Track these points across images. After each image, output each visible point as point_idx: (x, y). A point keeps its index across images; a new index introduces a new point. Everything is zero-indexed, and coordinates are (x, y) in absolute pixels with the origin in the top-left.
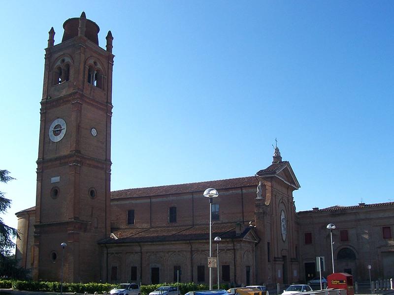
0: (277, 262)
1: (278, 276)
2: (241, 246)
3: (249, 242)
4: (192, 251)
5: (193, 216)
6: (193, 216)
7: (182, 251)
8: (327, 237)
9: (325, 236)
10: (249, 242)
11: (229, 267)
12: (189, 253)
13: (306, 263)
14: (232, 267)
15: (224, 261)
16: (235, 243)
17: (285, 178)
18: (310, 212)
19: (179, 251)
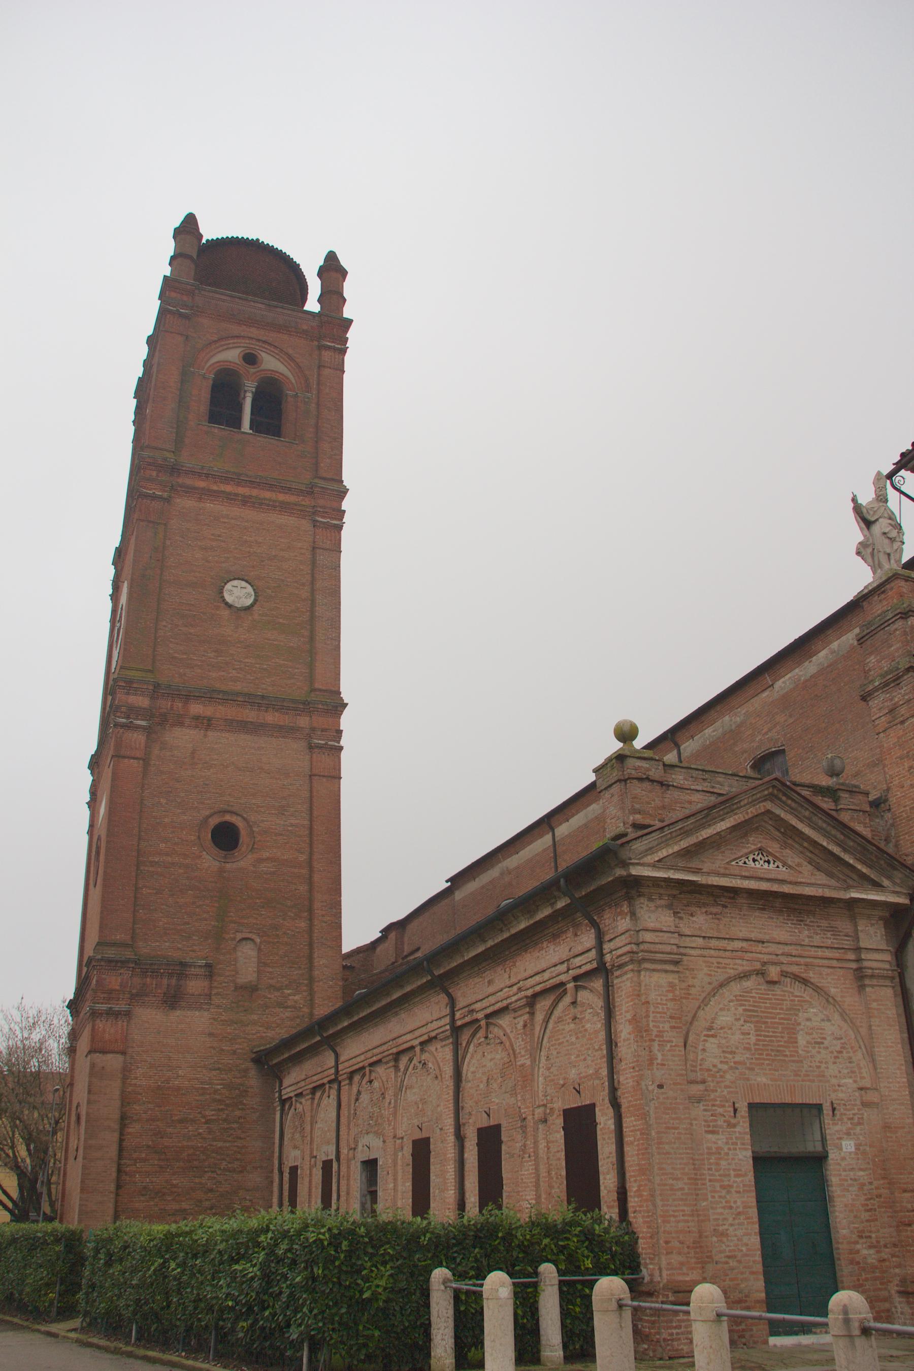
4: (456, 1031)
14: (605, 1120)
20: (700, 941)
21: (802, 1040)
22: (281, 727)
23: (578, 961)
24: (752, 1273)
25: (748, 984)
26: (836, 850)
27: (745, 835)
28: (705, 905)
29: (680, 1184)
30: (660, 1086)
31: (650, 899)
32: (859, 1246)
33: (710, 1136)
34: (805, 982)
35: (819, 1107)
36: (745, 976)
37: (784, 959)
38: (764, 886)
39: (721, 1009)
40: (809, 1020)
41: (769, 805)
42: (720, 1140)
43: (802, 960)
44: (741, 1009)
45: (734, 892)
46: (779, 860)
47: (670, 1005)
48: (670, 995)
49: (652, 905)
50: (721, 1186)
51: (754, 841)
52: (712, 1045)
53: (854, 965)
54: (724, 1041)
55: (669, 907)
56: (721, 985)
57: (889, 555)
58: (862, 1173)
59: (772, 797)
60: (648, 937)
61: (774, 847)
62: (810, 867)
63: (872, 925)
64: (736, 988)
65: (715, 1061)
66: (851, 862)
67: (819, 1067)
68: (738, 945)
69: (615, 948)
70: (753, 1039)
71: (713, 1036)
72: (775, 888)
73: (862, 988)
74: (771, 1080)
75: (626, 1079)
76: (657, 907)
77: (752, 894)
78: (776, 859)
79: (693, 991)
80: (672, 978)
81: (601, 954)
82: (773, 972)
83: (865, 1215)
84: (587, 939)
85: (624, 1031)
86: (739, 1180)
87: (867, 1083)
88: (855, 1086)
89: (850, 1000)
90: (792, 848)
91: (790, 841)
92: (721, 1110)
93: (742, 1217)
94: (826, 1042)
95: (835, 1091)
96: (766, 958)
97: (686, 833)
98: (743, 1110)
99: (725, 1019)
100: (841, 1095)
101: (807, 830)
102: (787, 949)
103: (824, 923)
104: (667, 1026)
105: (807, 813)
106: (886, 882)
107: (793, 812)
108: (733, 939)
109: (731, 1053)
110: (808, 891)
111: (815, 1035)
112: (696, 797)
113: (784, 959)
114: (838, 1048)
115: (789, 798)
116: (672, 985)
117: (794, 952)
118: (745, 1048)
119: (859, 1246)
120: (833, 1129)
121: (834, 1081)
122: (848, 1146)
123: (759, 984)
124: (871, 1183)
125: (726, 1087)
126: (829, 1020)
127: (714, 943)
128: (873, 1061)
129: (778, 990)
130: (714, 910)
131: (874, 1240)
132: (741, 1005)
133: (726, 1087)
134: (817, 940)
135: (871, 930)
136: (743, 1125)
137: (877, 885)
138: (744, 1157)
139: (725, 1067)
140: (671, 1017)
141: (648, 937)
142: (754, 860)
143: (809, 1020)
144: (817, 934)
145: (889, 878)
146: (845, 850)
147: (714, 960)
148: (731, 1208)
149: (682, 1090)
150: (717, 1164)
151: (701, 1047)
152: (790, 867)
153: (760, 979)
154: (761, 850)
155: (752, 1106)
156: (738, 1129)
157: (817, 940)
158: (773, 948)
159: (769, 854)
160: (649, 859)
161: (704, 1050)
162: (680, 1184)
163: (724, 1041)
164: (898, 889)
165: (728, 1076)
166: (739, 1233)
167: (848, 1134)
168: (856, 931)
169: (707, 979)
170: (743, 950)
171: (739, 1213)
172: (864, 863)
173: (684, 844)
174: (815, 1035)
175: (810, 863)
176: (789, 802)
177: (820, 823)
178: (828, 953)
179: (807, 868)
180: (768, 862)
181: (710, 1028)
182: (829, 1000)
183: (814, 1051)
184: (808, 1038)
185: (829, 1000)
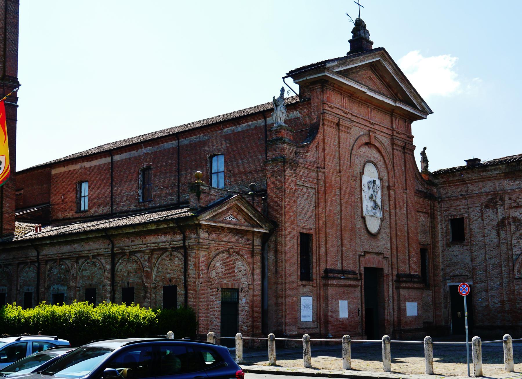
0: (331, 282)
1: (338, 312)
2: (199, 238)
3: (237, 232)
5: (178, 186)
6: (178, 186)
7: (98, 255)
8: (498, 225)
9: (495, 224)
10: (237, 232)
11: (176, 291)
12: (109, 261)
13: (450, 286)
14: (180, 290)
15: (168, 276)
16: (187, 233)
17: (384, 91)
18: (461, 169)
19: (94, 257)
21: (236, 271)
23: (174, 243)
24: (218, 333)
26: (252, 216)
28: (215, 231)
29: (204, 310)
30: (201, 283)
31: (203, 230)
32: (243, 326)
33: (211, 297)
34: (239, 254)
35: (238, 289)
36: (223, 252)
37: (234, 247)
38: (232, 226)
39: (217, 262)
40: (238, 265)
41: (236, 202)
42: (213, 298)
43: (238, 248)
44: (222, 262)
46: (236, 218)
47: (205, 260)
48: (205, 258)
49: (203, 231)
50: (213, 310)
52: (214, 272)
53: (251, 250)
54: (217, 271)
55: (207, 232)
57: (281, 118)
58: (246, 307)
59: (237, 200)
61: (235, 214)
62: (244, 220)
63: (258, 238)
64: (221, 255)
65: (214, 276)
66: (256, 220)
67: (239, 278)
68: (223, 243)
69: (190, 242)
70: (224, 270)
71: (214, 269)
73: (252, 256)
74: (228, 282)
75: (191, 280)
76: (204, 232)
77: (228, 228)
79: (211, 256)
80: (206, 253)
81: (184, 243)
82: (231, 251)
83: (246, 318)
84: (179, 237)
85: (191, 267)
86: (217, 308)
87: (250, 283)
88: (248, 284)
90: (240, 214)
91: (240, 213)
92: (214, 290)
93: (217, 318)
94: (242, 272)
95: (242, 285)
98: (220, 290)
100: (244, 286)
101: (245, 210)
102: (235, 244)
103: (245, 237)
104: (204, 266)
105: (246, 205)
106: (264, 226)
108: (222, 242)
109: (218, 274)
110: (243, 228)
111: (239, 270)
112: (217, 198)
113: (234, 247)
114: (245, 273)
115: (242, 200)
116: (206, 255)
117: (237, 246)
118: (222, 273)
119: (243, 326)
120: (241, 295)
121: (242, 282)
122: (244, 300)
123: (227, 255)
124: (248, 310)
125: (216, 283)
126: (243, 265)
127: (217, 242)
128: (253, 277)
130: (218, 233)
131: (247, 325)
132: (222, 261)
133: (216, 283)
134: (243, 241)
135: (257, 239)
136: (219, 294)
137: (261, 227)
138: (219, 302)
139: (216, 278)
140: (205, 264)
142: (230, 218)
143: (238, 265)
144: (243, 240)
145: (265, 225)
146: (254, 216)
147: (216, 247)
148: (215, 316)
149: (206, 284)
150: (212, 304)
151: (211, 272)
152: (239, 220)
154: (232, 215)
155: (222, 289)
156: (218, 295)
159: (234, 216)
161: (212, 273)
162: (204, 310)
163: (217, 271)
164: (267, 228)
165: (217, 281)
166: (216, 322)
167: (244, 297)
168: (253, 240)
169: (214, 253)
170: (224, 245)
171: (216, 317)
172: (259, 220)
174: (239, 270)
175: (244, 219)
176: (242, 202)
177: (249, 208)
179: (243, 220)
180: (233, 218)
181: (214, 267)
183: (238, 274)
184: (237, 270)
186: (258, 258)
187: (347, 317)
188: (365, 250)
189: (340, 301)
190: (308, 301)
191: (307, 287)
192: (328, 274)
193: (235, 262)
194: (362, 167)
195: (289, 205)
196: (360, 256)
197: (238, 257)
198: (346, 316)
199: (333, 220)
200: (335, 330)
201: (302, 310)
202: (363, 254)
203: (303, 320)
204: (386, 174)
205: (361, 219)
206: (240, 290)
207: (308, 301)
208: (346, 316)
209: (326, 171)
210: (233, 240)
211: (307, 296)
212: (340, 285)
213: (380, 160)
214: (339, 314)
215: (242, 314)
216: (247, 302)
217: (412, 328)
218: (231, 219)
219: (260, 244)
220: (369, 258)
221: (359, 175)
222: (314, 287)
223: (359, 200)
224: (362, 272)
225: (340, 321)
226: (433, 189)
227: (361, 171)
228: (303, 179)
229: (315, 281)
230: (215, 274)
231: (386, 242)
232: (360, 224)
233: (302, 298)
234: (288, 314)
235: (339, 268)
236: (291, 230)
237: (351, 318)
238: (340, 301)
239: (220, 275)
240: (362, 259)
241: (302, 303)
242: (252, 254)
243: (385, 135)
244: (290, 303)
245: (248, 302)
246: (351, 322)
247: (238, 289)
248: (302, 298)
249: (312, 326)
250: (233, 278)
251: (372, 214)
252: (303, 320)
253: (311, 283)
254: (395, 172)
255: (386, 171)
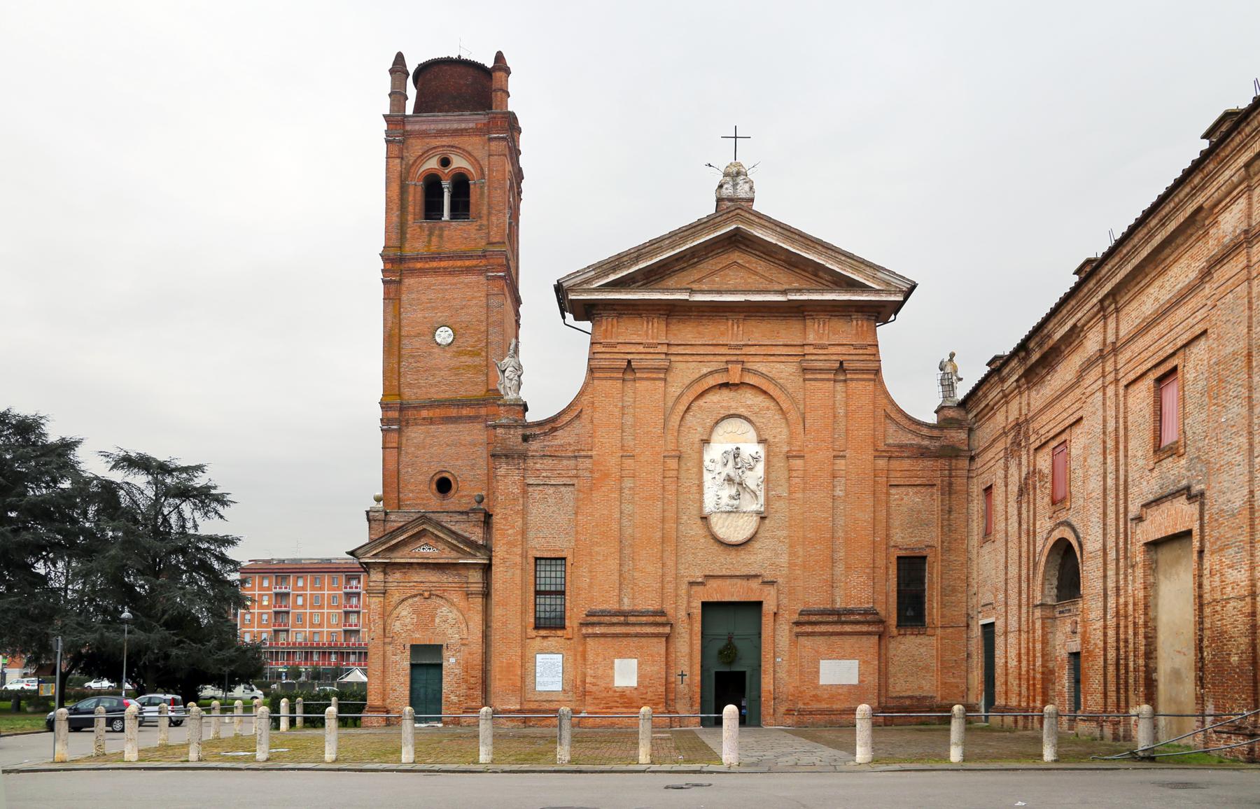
20: (396, 584)
21: (437, 620)
22: (470, 417)
25: (416, 599)
26: (455, 542)
27: (419, 539)
35: (442, 646)
36: (415, 596)
38: (420, 561)
42: (398, 658)
45: (411, 564)
51: (423, 541)
52: (398, 623)
56: (403, 600)
60: (371, 584)
64: (410, 601)
72: (426, 561)
77: (418, 564)
78: (433, 547)
87: (465, 637)
89: (463, 604)
96: (424, 589)
97: (384, 543)
98: (408, 646)
99: (404, 613)
101: (442, 535)
102: (434, 584)
103: (455, 572)
106: (478, 554)
107: (434, 528)
120: (445, 653)
122: (452, 660)
127: (401, 584)
129: (429, 601)
134: (450, 580)
135: (475, 574)
136: (408, 653)
137: (474, 556)
138: (406, 664)
141: (371, 584)
153: (422, 597)
155: (412, 646)
157: (450, 580)
158: (427, 584)
160: (368, 555)
172: (467, 547)
173: (384, 547)
178: (454, 585)
182: (453, 604)
185: (453, 604)
186: (476, 600)
187: (635, 685)
188: (707, 573)
189: (617, 661)
190: (552, 661)
191: (550, 639)
192: (594, 618)
193: (435, 608)
194: (708, 430)
195: (506, 519)
196: (691, 584)
197: (439, 601)
198: (633, 682)
199: (611, 530)
200: (602, 706)
201: (537, 675)
202: (700, 580)
203: (539, 688)
204: (785, 431)
205: (699, 521)
206: (445, 647)
207: (552, 661)
208: (633, 682)
209: (595, 453)
210: (434, 579)
211: (552, 653)
212: (614, 634)
213: (768, 409)
214: (613, 680)
215: (449, 679)
216: (457, 662)
217: (835, 707)
218: (426, 551)
219: (481, 580)
220: (719, 586)
221: (696, 446)
222: (568, 639)
223: (694, 489)
224: (697, 611)
225: (615, 691)
226: (953, 434)
227: (705, 438)
228: (544, 474)
229: (569, 630)
230: (399, 626)
231: (777, 555)
232: (697, 529)
233: (539, 657)
234: (499, 679)
235: (616, 607)
236: (508, 556)
237: (646, 687)
238: (617, 661)
239: (408, 628)
240: (695, 588)
241: (538, 664)
242: (468, 595)
243: (783, 359)
244: (505, 664)
245: (459, 663)
246: (647, 693)
247: (442, 646)
248: (539, 657)
249: (561, 697)
250: (432, 631)
251: (729, 509)
252: (539, 688)
253: (560, 633)
254: (807, 422)
255: (783, 425)
